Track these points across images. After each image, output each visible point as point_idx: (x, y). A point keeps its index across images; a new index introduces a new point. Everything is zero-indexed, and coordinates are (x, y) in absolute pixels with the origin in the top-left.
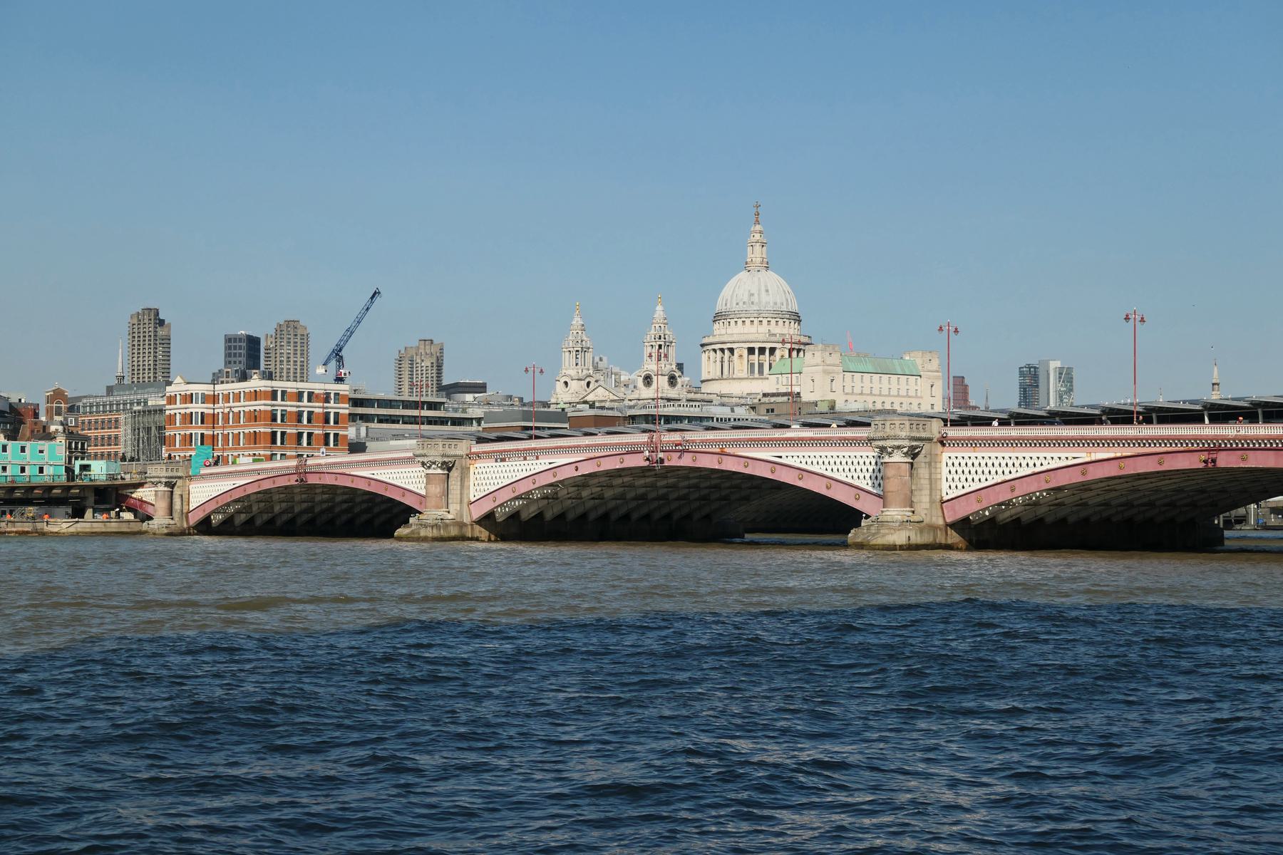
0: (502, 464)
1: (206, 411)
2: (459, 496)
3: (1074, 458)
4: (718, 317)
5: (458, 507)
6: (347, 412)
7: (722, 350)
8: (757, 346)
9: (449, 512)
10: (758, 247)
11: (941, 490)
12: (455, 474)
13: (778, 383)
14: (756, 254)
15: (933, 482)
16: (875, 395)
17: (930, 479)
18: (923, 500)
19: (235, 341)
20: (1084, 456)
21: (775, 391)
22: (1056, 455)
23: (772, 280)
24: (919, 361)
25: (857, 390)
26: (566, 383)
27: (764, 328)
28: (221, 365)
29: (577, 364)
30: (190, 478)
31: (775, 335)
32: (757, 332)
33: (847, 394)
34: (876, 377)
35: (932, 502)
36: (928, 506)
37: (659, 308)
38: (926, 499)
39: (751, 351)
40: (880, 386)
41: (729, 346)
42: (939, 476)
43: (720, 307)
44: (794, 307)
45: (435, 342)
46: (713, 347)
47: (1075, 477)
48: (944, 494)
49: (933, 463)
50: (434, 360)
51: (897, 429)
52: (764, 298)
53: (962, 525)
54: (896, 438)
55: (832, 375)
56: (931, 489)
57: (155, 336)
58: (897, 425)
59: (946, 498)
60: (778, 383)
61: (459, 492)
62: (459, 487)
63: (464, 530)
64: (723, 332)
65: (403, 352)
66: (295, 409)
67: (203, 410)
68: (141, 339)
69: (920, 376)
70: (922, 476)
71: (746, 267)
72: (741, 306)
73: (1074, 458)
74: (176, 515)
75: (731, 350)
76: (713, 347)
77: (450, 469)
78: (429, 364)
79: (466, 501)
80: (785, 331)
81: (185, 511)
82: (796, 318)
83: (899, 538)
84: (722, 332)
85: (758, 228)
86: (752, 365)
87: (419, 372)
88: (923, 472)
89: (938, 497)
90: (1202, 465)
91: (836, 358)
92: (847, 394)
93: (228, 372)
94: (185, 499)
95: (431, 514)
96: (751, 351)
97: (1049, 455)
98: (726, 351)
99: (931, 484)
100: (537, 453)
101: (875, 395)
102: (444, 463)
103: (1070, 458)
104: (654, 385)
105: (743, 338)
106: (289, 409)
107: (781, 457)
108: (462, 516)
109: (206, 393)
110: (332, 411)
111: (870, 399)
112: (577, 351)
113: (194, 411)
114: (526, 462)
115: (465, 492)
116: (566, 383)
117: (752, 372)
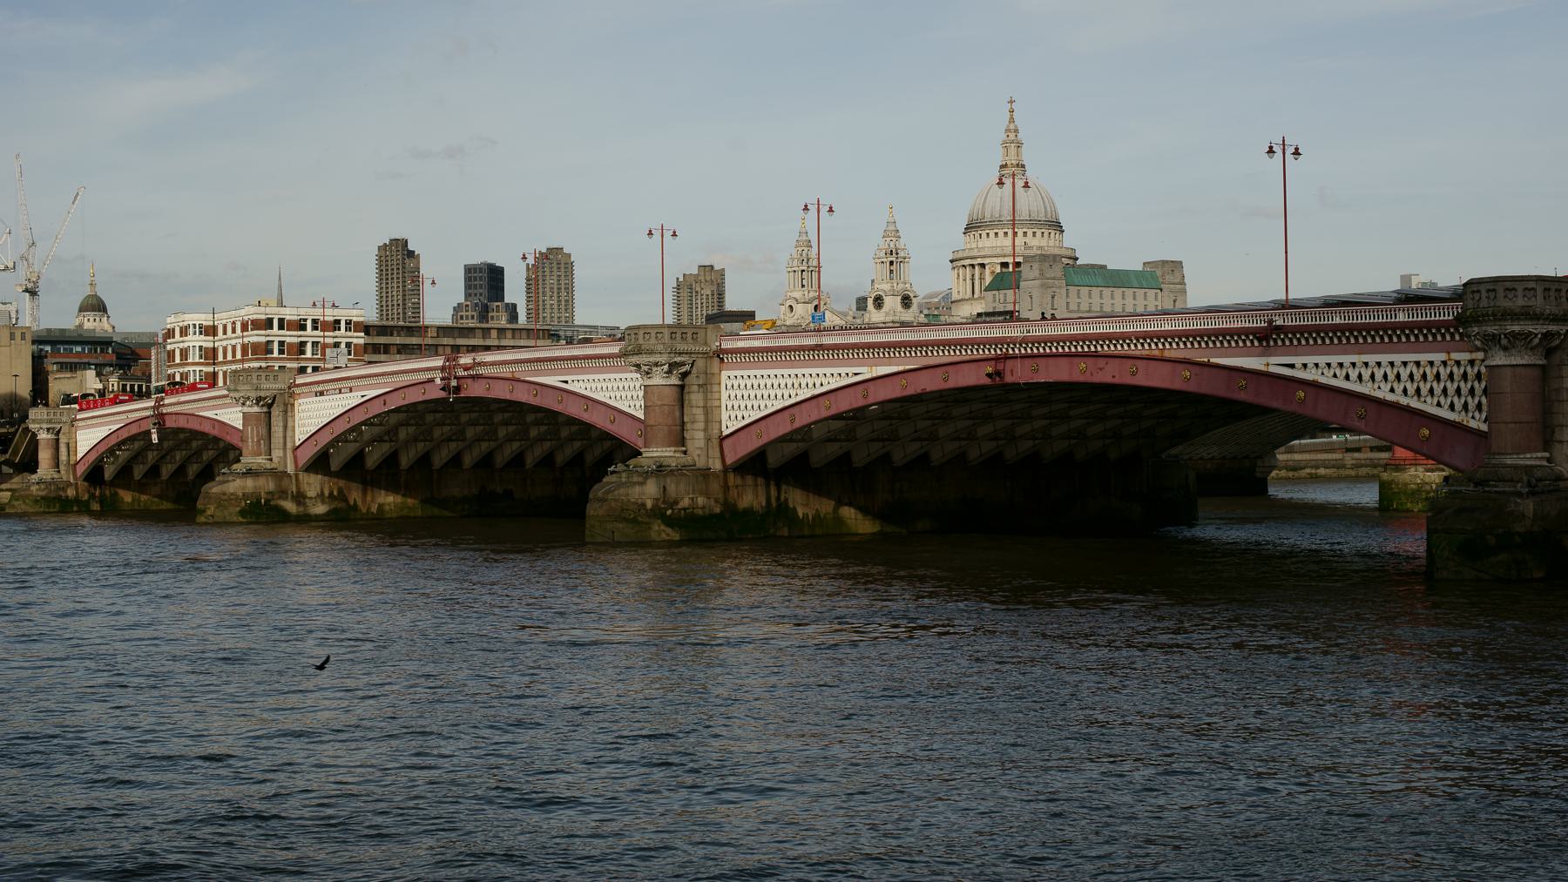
1: (205, 345)
2: (281, 440)
3: (856, 374)
5: (281, 453)
6: (362, 341)
9: (271, 460)
11: (720, 422)
13: (995, 301)
15: (710, 413)
17: (705, 407)
18: (696, 438)
19: (475, 272)
20: (867, 372)
21: (991, 310)
22: (835, 371)
25: (1085, 307)
26: (791, 307)
28: (462, 300)
29: (803, 286)
31: (1031, 247)
35: (708, 440)
36: (701, 443)
38: (701, 435)
40: (1146, 303)
41: (980, 261)
42: (716, 403)
45: (716, 268)
46: (963, 262)
47: (845, 404)
49: (709, 385)
50: (715, 288)
51: (653, 341)
54: (651, 352)
55: (1054, 289)
56: (707, 421)
57: (404, 268)
58: (653, 335)
59: (726, 432)
60: (995, 301)
61: (281, 435)
62: (281, 429)
63: (285, 482)
64: (974, 246)
65: (681, 279)
66: (296, 340)
67: (201, 344)
68: (390, 272)
69: (1161, 290)
70: (694, 403)
73: (856, 374)
74: (62, 468)
76: (963, 262)
77: (270, 406)
78: (709, 293)
79: (289, 445)
80: (1044, 243)
81: (72, 462)
87: (699, 301)
88: (695, 398)
89: (716, 431)
90: (988, 381)
93: (467, 306)
95: (249, 460)
97: (828, 371)
98: (977, 267)
99: (706, 414)
102: (259, 400)
103: (850, 375)
104: (884, 310)
105: (998, 251)
106: (288, 340)
107: (566, 382)
108: (286, 467)
109: (204, 323)
110: (277, 339)
112: (803, 271)
113: (191, 344)
115: (289, 433)
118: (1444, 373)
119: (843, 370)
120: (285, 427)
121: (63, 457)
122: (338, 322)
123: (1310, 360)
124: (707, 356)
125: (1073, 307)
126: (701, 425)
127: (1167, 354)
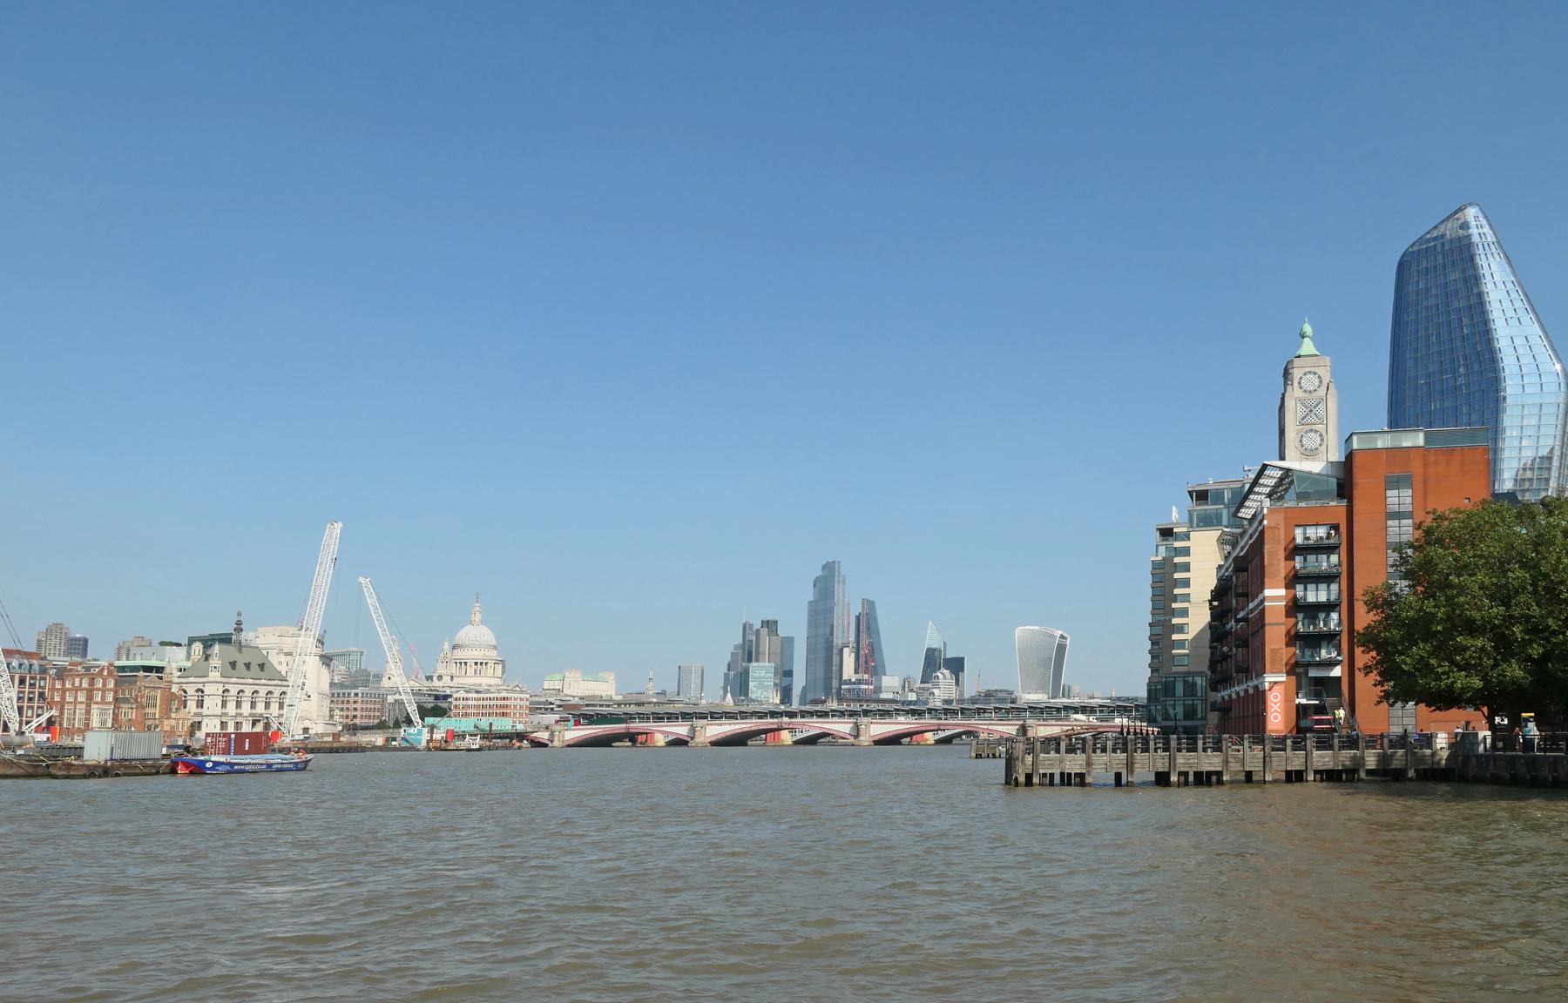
4: (454, 647)
7: (461, 663)
8: (479, 661)
10: (477, 614)
14: (477, 618)
23: (485, 630)
24: (606, 676)
26: (389, 678)
27: (482, 653)
30: (566, 730)
32: (478, 654)
37: (446, 644)
39: (476, 663)
43: (455, 643)
44: (495, 644)
52: (483, 638)
53: (874, 741)
71: (471, 623)
72: (471, 642)
75: (466, 663)
82: (495, 648)
83: (866, 744)
84: (458, 654)
85: (478, 605)
86: (475, 670)
91: (579, 675)
94: (563, 737)
96: (476, 663)
98: (463, 664)
116: (389, 678)
117: (475, 673)
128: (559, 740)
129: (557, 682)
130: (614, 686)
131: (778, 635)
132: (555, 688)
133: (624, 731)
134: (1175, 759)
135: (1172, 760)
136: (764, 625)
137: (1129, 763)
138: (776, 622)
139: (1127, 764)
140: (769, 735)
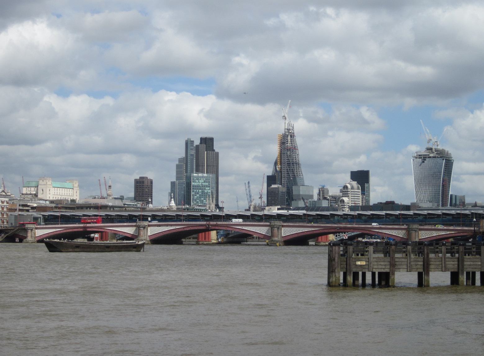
0: (159, 227)
12: (145, 229)
13: (27, 190)
15: (281, 233)
16: (66, 196)
21: (25, 193)
33: (53, 195)
34: (61, 189)
35: (281, 237)
38: (280, 236)
48: (283, 235)
49: (281, 230)
55: (50, 188)
69: (73, 189)
88: (280, 231)
92: (53, 195)
94: (35, 234)
97: (306, 229)
100: (171, 225)
101: (66, 196)
111: (55, 196)
114: (167, 227)
118: (401, 233)
119: (309, 229)
120: (147, 232)
121: (33, 235)
122: (4, 201)
123: (385, 231)
124: (280, 225)
125: (56, 194)
126: (280, 235)
127: (365, 229)
128: (32, 237)
129: (33, 189)
130: (78, 192)
131: (214, 150)
132: (32, 193)
133: (81, 230)
134: (463, 261)
135: (460, 262)
136: (203, 142)
137: (426, 264)
138: (211, 140)
139: (424, 265)
140: (200, 234)
